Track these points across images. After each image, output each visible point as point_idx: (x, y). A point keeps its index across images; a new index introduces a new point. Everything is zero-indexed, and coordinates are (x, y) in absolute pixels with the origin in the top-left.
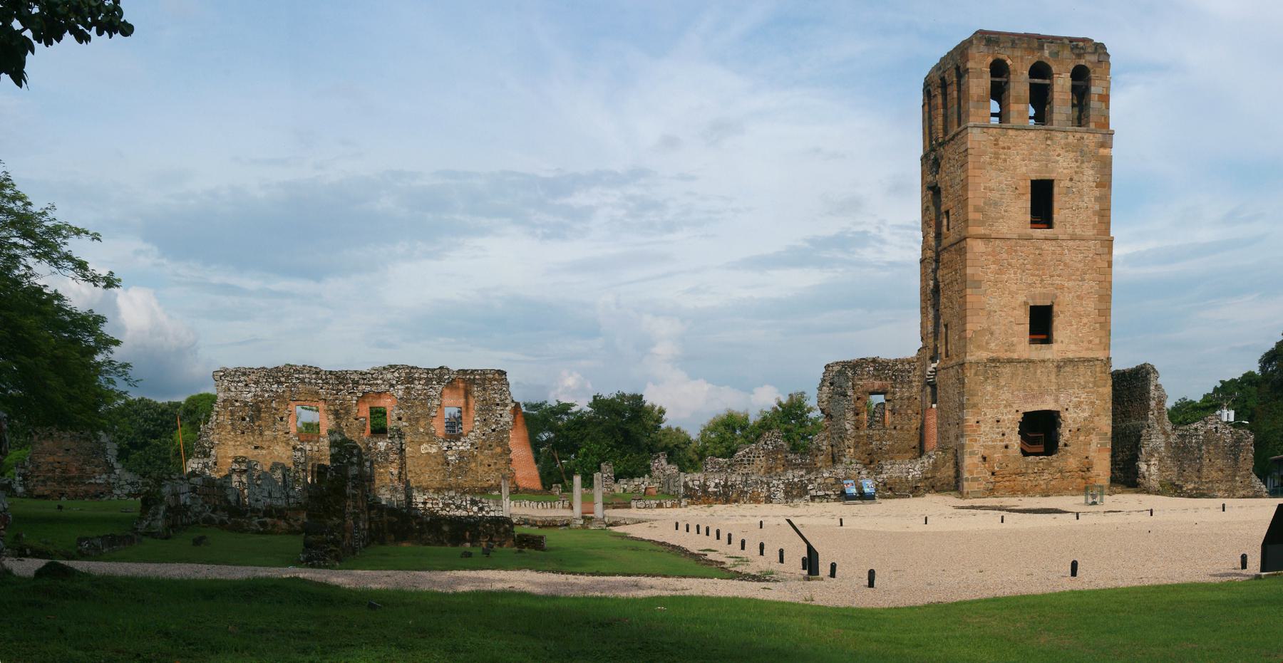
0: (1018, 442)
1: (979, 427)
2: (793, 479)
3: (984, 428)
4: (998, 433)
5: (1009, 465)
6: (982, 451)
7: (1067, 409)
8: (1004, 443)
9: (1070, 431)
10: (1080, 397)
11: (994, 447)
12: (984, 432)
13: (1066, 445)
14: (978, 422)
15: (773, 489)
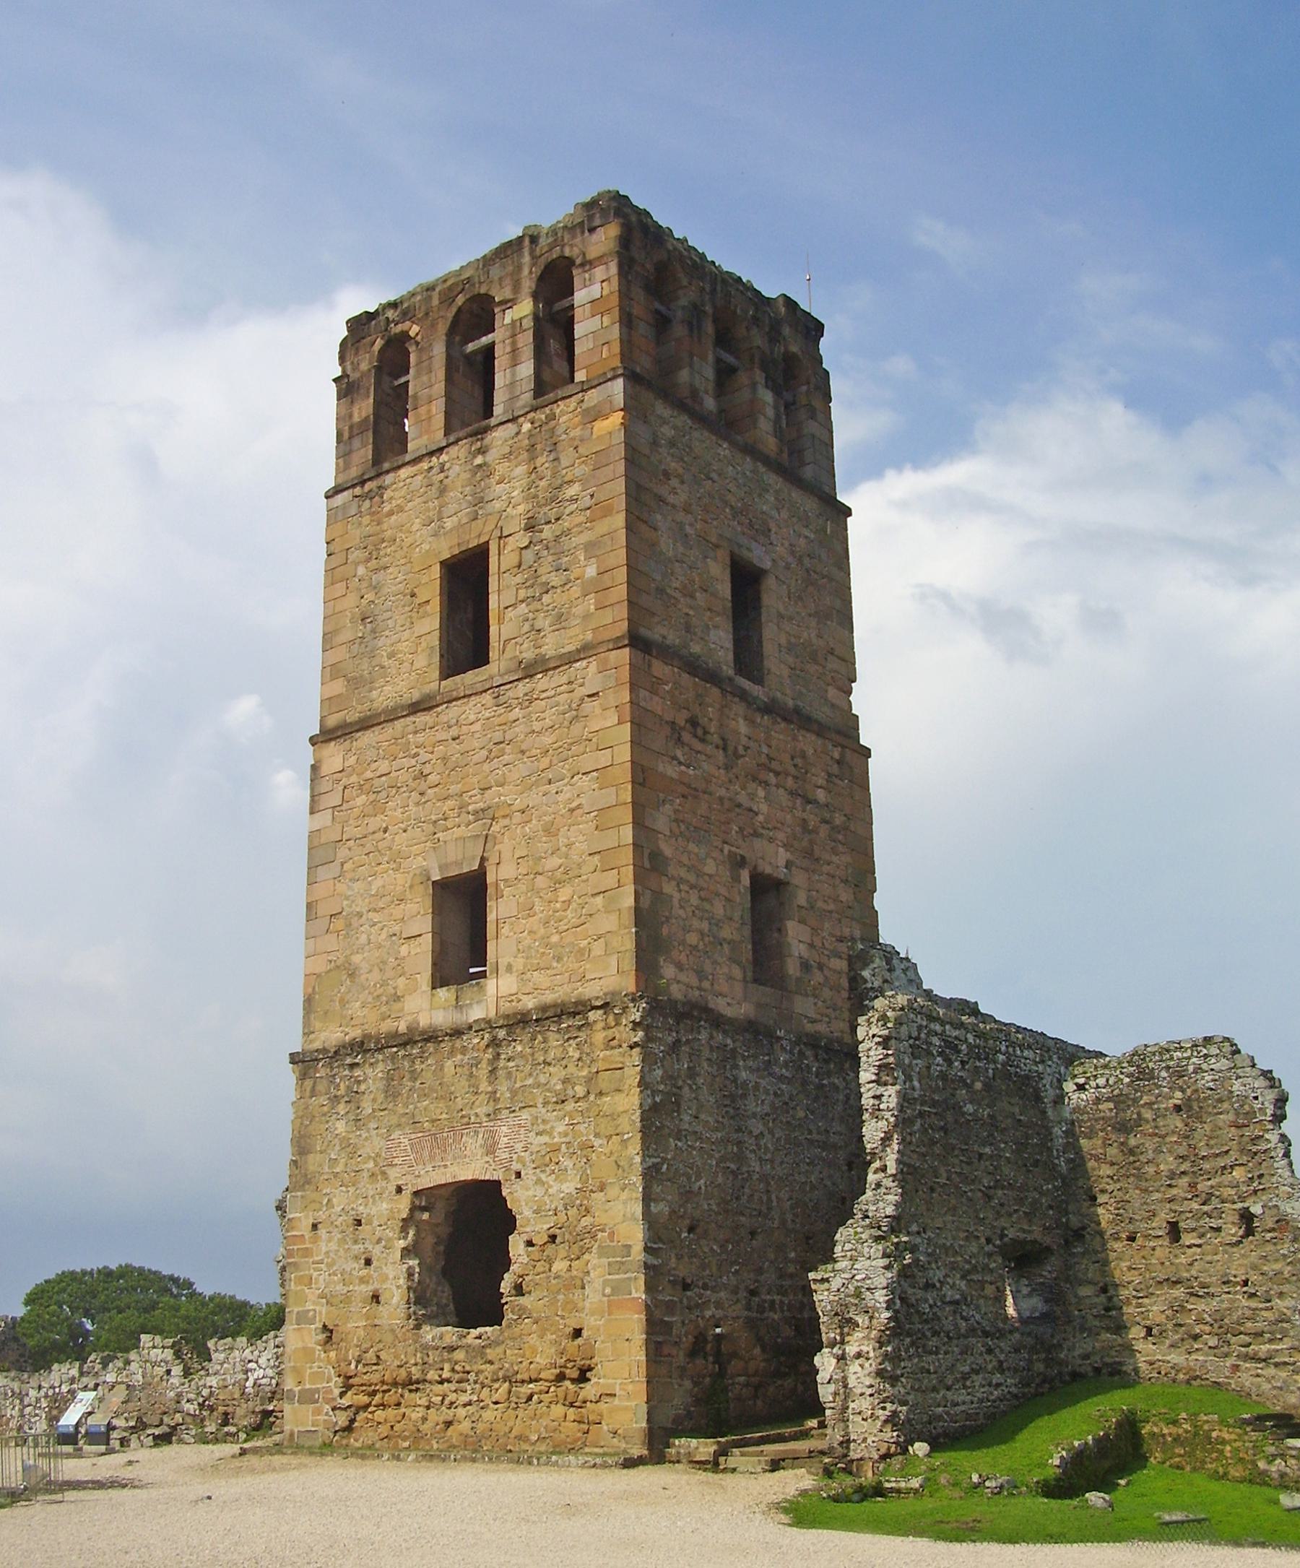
0: (402, 1281)
1: (315, 1240)
2: (60, 1386)
3: (327, 1244)
4: (356, 1258)
5: (383, 1355)
6: (323, 1313)
7: (518, 1175)
8: (371, 1288)
9: (530, 1243)
10: (550, 1133)
11: (347, 1298)
12: (327, 1253)
13: (519, 1290)
14: (315, 1227)
15: (28, 1410)
